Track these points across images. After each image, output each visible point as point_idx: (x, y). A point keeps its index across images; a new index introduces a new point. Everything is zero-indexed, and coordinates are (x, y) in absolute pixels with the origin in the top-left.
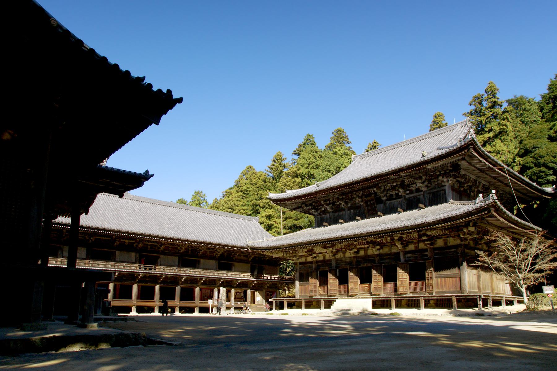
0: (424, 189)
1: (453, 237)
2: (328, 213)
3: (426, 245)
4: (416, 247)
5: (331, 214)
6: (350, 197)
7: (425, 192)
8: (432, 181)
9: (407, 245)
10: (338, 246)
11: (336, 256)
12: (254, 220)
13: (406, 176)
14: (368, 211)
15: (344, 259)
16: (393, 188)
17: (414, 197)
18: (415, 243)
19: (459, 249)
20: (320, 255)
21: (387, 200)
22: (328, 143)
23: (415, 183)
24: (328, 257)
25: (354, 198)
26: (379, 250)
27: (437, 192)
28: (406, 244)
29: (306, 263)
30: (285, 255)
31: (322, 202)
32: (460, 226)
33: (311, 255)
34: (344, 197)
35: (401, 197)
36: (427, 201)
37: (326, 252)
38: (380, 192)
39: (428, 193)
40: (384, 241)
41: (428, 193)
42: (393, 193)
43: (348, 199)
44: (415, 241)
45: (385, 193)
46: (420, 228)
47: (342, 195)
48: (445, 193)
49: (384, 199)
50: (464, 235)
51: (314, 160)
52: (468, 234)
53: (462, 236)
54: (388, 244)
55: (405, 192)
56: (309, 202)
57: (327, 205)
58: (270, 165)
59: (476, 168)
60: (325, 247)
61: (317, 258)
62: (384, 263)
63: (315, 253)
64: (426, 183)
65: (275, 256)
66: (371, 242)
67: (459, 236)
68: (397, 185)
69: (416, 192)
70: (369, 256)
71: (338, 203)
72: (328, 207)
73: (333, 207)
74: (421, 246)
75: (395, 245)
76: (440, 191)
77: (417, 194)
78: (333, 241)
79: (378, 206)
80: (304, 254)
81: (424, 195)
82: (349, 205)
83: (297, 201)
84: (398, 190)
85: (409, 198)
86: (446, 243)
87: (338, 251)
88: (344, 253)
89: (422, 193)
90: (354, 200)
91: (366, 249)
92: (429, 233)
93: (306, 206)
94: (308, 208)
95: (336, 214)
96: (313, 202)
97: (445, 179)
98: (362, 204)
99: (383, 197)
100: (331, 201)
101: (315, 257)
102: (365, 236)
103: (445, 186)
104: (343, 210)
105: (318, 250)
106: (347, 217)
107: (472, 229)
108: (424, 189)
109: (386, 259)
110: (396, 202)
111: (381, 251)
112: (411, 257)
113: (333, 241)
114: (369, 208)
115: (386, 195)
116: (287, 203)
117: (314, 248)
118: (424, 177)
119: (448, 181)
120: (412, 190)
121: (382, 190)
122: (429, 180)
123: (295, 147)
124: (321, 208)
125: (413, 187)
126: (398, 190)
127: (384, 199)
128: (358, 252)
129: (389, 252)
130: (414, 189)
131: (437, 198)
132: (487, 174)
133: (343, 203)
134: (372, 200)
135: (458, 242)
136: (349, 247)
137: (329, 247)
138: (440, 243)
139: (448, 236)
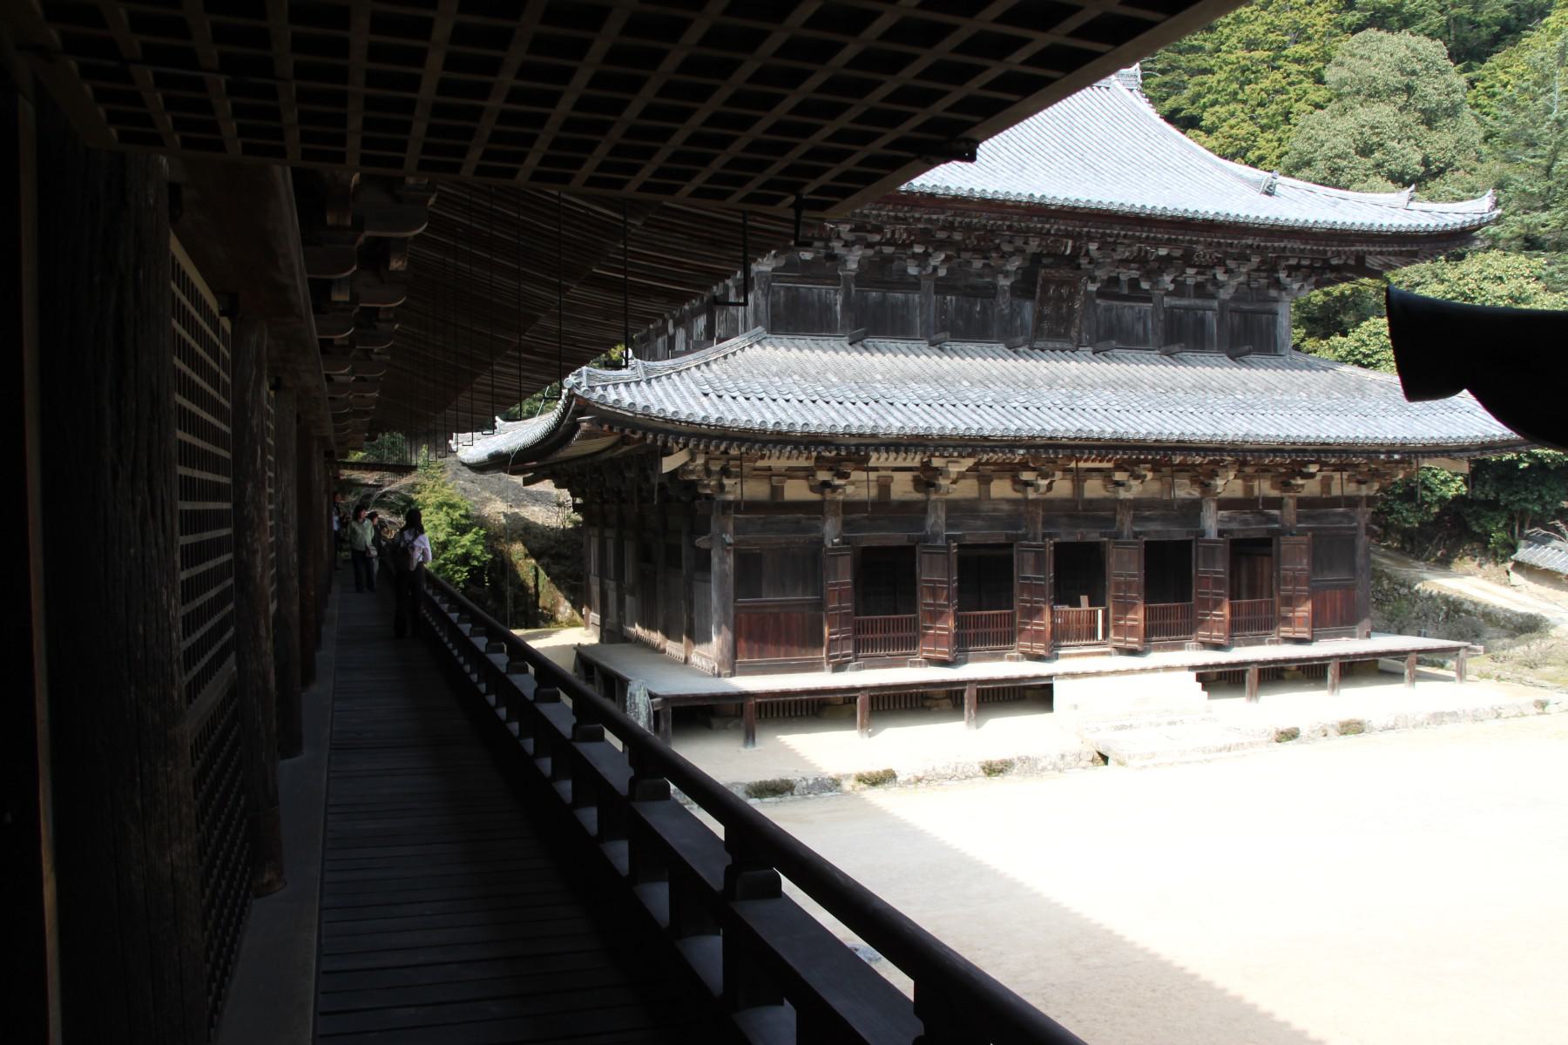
7: (1223, 304)
15: (985, 506)
17: (1187, 309)
27: (1253, 312)
35: (1146, 297)
68: (1169, 259)
69: (1198, 296)
70: (1090, 501)
76: (1264, 312)
77: (1199, 302)
85: (1172, 308)
86: (1326, 483)
88: (985, 480)
89: (1215, 304)
90: (966, 255)
98: (1004, 282)
103: (1276, 300)
110: (1130, 311)
112: (1231, 519)
114: (1047, 311)
130: (1190, 281)
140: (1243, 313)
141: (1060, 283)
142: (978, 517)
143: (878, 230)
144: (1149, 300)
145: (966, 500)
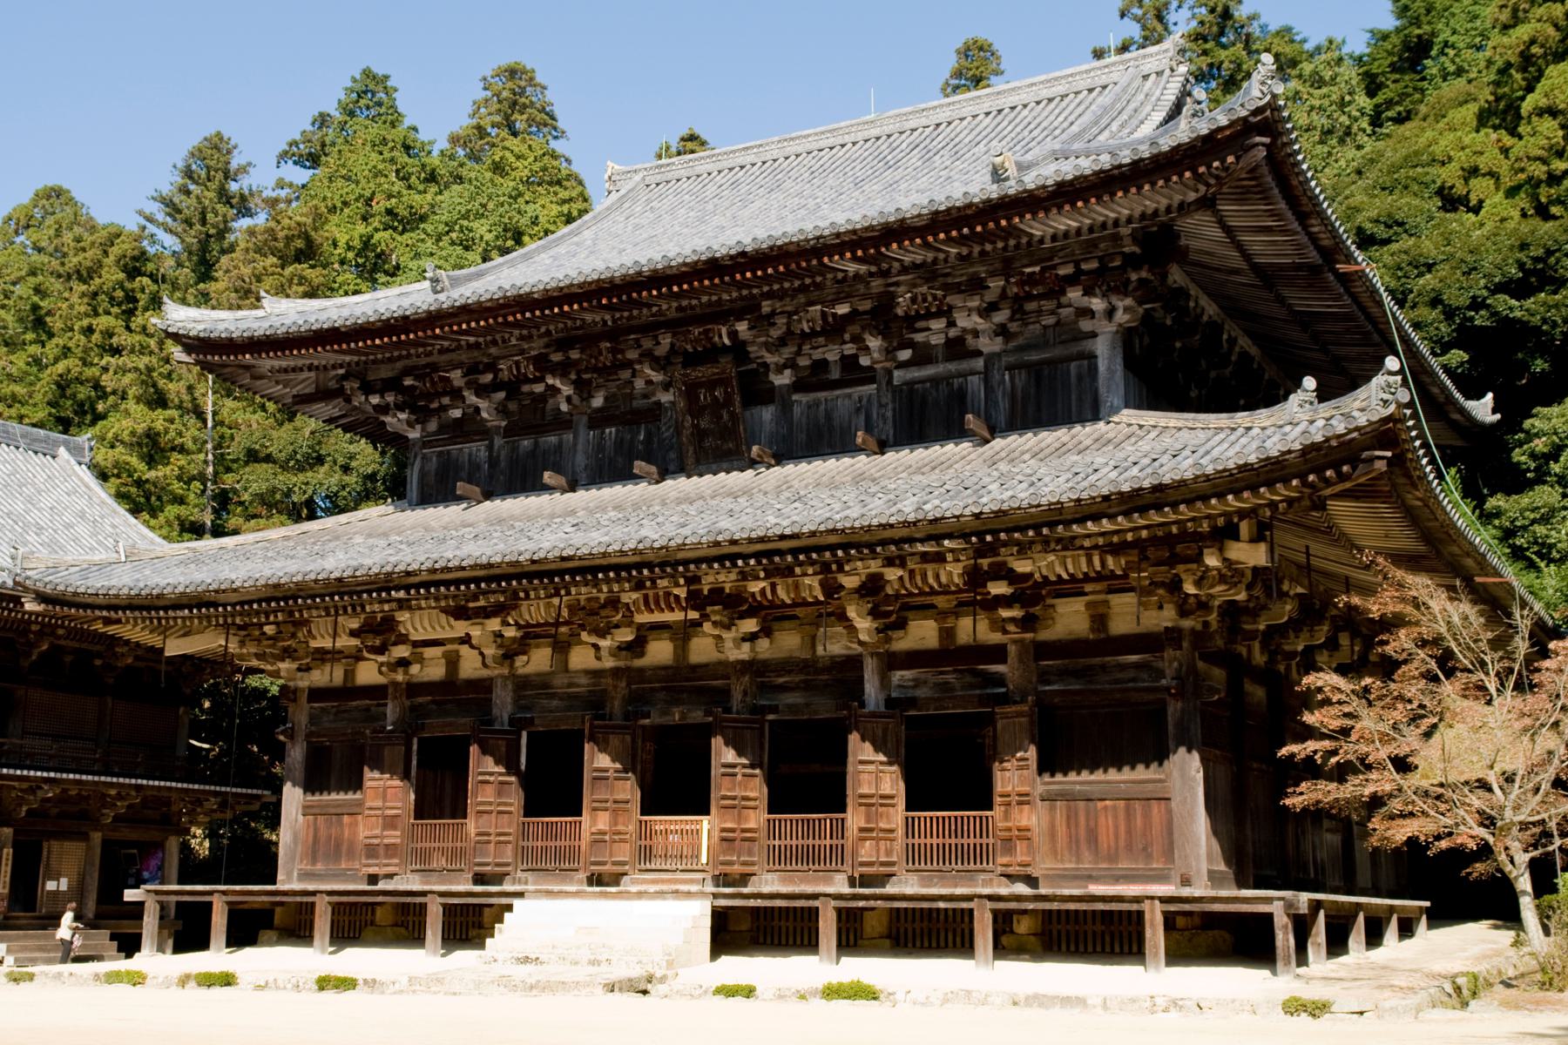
0: (989, 345)
1: (1144, 592)
2: (484, 432)
3: (1000, 625)
4: (947, 634)
5: (498, 441)
6: (606, 359)
7: (991, 359)
8: (1031, 306)
9: (901, 625)
10: (535, 610)
11: (520, 660)
12: (62, 451)
13: (915, 266)
14: (699, 434)
15: (559, 681)
16: (834, 329)
17: (935, 381)
18: (941, 615)
19: (1169, 653)
20: (429, 652)
21: (798, 386)
22: (461, 121)
23: (946, 312)
24: (470, 666)
25: (629, 364)
26: (751, 638)
28: (892, 612)
29: (349, 691)
30: (233, 647)
31: (456, 377)
32: (1198, 537)
33: (381, 650)
34: (575, 355)
35: (868, 376)
36: (1003, 404)
37: (466, 640)
38: (766, 345)
39: (1010, 368)
40: (782, 593)
41: (1010, 368)
42: (832, 354)
43: (595, 370)
44: (941, 602)
45: (787, 352)
46: (991, 535)
47: (563, 344)
48: (1093, 370)
49: (783, 379)
50: (1198, 584)
51: (399, 186)
52: (1222, 579)
53: (1190, 589)
54: (799, 611)
55: (889, 352)
56: (385, 372)
57: (482, 391)
58: (166, 190)
59: (1246, 256)
60: (460, 613)
61: (415, 669)
62: (774, 709)
63: (403, 639)
64: (1000, 317)
65: (175, 647)
66: (717, 595)
67: (1175, 586)
70: (695, 668)
71: (539, 388)
72: (483, 404)
73: (512, 406)
74: (972, 629)
75: (842, 617)
76: (1071, 359)
77: (952, 367)
78: (519, 577)
79: (748, 413)
80: (345, 642)
81: (986, 374)
82: (598, 402)
83: (323, 356)
84: (857, 339)
85: (910, 384)
86: (1099, 619)
87: (531, 635)
88: (562, 648)
89: (979, 363)
90: (625, 374)
91: (683, 634)
92: (1022, 567)
93: (368, 389)
94: (375, 400)
95: (526, 443)
96: (407, 372)
97: (1097, 304)
98: (665, 398)
99: (780, 369)
100: (504, 376)
101: (403, 663)
102: (698, 561)
103: (1094, 335)
104: (563, 423)
105: (420, 624)
106: (581, 460)
107: (1249, 554)
108: (989, 345)
109: (784, 688)
110: (843, 400)
111: (763, 644)
112: (917, 683)
113: (519, 577)
114: (704, 424)
115: (791, 364)
116: (267, 363)
117: (403, 616)
118: (996, 284)
119: (1110, 313)
120: (927, 345)
121: (775, 333)
122: (1016, 297)
123: (298, 124)
124: (444, 408)
125: (935, 333)
126: (857, 339)
127: (783, 379)
128: (636, 647)
129: (806, 655)
131: (1049, 395)
132: (1281, 300)
133: (567, 390)
134: (723, 382)
135: (1166, 617)
136: (596, 618)
137: (486, 613)
138: (1070, 618)
139: (1117, 584)
140: (1028, 366)
141: (711, 385)
142: (553, 696)
143: (492, 367)
144: (872, 380)
145: (538, 675)
